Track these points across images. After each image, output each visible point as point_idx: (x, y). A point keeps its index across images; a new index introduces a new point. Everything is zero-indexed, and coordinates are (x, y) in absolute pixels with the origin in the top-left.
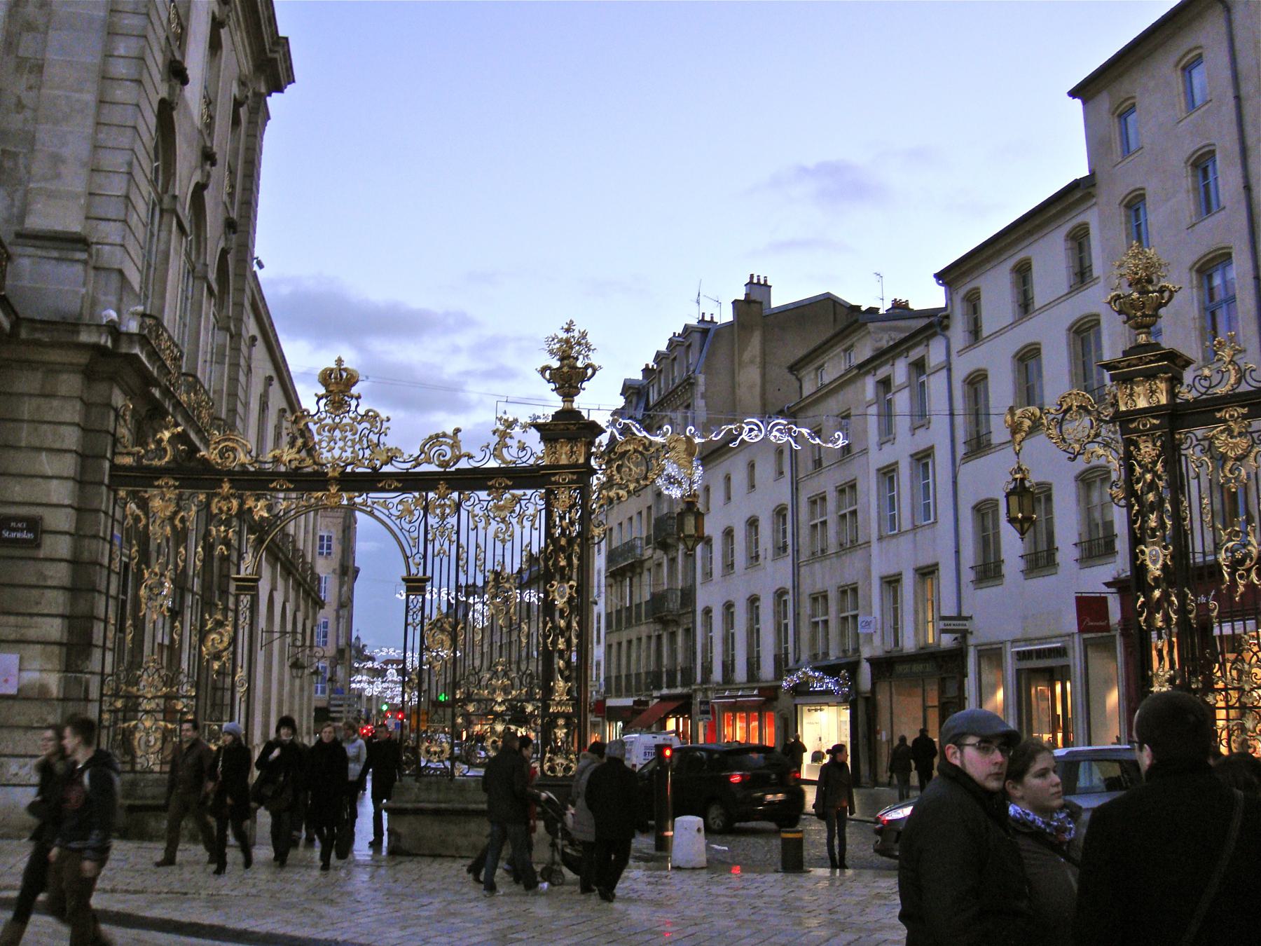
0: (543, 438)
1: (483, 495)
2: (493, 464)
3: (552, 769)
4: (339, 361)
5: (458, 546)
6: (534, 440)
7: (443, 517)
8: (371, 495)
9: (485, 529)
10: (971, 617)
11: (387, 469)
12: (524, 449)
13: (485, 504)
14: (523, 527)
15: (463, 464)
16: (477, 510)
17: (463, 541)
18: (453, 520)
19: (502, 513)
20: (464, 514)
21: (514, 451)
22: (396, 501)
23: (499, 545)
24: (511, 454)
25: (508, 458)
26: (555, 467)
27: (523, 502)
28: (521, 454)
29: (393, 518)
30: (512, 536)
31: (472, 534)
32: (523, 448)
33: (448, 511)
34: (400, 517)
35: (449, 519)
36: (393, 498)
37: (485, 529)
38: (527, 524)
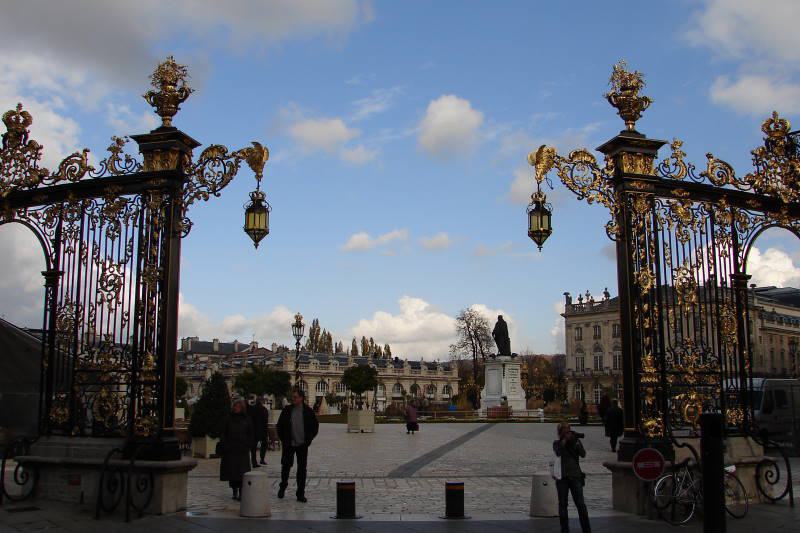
0: (142, 150)
1: (100, 201)
2: (107, 175)
3: (414, 389)
4: (20, 106)
5: (81, 244)
6: (132, 149)
7: (71, 222)
8: (30, 208)
9: (101, 227)
11: (41, 186)
13: (100, 207)
14: (127, 226)
15: (86, 177)
16: (96, 214)
18: (78, 223)
19: (109, 213)
20: (86, 217)
21: (122, 163)
22: (42, 211)
23: (109, 240)
24: (121, 166)
25: (119, 169)
26: (153, 175)
27: (129, 204)
28: (128, 165)
29: (40, 225)
31: (91, 232)
32: (128, 160)
33: (76, 215)
34: (44, 224)
35: (75, 222)
36: (41, 209)
37: (101, 227)
38: (130, 222)
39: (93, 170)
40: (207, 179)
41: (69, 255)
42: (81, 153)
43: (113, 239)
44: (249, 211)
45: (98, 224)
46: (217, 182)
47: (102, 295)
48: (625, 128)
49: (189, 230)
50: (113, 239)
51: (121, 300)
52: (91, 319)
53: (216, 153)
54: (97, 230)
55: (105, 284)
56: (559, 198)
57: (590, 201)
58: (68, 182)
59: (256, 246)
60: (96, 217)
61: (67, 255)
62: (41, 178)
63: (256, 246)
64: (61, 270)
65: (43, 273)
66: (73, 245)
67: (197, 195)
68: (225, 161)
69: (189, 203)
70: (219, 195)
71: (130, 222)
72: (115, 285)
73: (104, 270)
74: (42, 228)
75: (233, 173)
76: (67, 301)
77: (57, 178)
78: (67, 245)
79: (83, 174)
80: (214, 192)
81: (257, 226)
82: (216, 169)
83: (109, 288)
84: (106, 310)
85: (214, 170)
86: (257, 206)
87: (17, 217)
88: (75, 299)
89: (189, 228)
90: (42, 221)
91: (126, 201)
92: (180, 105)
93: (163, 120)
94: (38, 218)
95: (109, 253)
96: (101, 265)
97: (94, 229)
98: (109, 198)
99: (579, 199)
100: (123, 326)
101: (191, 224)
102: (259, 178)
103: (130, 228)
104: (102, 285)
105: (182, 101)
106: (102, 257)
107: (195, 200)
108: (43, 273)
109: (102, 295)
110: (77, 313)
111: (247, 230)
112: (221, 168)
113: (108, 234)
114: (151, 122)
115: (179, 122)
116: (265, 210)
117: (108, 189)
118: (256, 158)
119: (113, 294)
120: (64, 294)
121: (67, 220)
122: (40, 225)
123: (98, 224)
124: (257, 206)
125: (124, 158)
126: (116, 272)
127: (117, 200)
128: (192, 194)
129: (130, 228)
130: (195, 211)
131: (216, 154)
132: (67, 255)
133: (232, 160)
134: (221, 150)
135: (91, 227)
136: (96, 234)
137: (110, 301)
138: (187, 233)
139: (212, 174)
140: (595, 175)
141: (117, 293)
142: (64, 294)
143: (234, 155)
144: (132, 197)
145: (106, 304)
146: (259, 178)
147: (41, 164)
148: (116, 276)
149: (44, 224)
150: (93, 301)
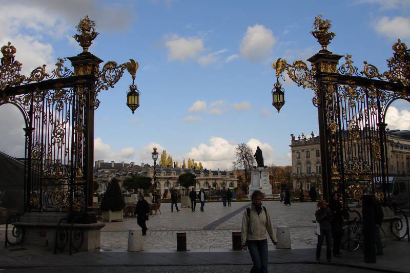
0: (73, 65)
1: (52, 91)
2: (56, 78)
3: (215, 185)
4: (9, 43)
5: (43, 113)
6: (68, 64)
7: (38, 102)
8: (16, 96)
9: (53, 105)
10: (292, 135)
11: (22, 84)
12: (67, 70)
14: (66, 104)
15: (45, 79)
16: (50, 98)
17: (45, 111)
18: (41, 103)
19: (57, 97)
20: (45, 100)
21: (63, 72)
24: (62, 73)
25: (62, 75)
27: (67, 93)
28: (66, 72)
29: (22, 105)
30: (63, 107)
31: (48, 107)
32: (66, 70)
33: (40, 99)
34: (24, 104)
35: (40, 103)
36: (22, 96)
37: (53, 105)
38: (68, 102)
39: (48, 75)
40: (107, 79)
41: (37, 120)
42: (42, 67)
43: (59, 111)
44: (129, 95)
45: (51, 104)
46: (112, 81)
47: (55, 140)
48: (322, 49)
49: (98, 105)
50: (59, 111)
51: (64, 142)
52: (49, 152)
53: (112, 65)
54: (51, 106)
55: (56, 134)
56: (288, 84)
57: (304, 87)
58: (35, 82)
59: (133, 113)
60: (50, 100)
61: (36, 119)
62: (22, 80)
63: (133, 113)
64: (33, 127)
65: (24, 129)
66: (39, 114)
67: (102, 87)
68: (116, 70)
69: (99, 91)
70: (113, 87)
71: (68, 102)
72: (61, 134)
73: (55, 127)
74: (23, 106)
75: (120, 75)
76: (37, 143)
77: (29, 80)
78: (36, 114)
79: (43, 78)
80: (111, 85)
81: (133, 103)
82: (111, 74)
83: (58, 136)
84: (57, 147)
85: (110, 74)
86: (133, 93)
87: (10, 101)
88: (40, 142)
89: (98, 104)
90: (23, 102)
91: (66, 91)
92: (92, 41)
93: (84, 49)
94: (21, 101)
95: (58, 118)
96: (53, 124)
97: (49, 106)
98: (57, 89)
99: (298, 86)
100: (65, 155)
101: (99, 102)
102: (134, 78)
103: (68, 105)
104: (54, 134)
105: (93, 39)
106: (54, 120)
107: (101, 90)
108: (24, 129)
109: (55, 140)
110: (42, 149)
111: (128, 105)
112: (114, 73)
113: (57, 109)
114: (78, 50)
115: (91, 50)
116: (137, 94)
117: (56, 85)
118: (132, 67)
119: (60, 139)
120: (35, 139)
121: (36, 101)
122: (22, 105)
123: (51, 104)
124: (133, 93)
125: (64, 69)
126: (61, 128)
127: (61, 91)
128: (99, 87)
129: (68, 105)
130: (102, 96)
131: (111, 66)
132: (36, 119)
133: (120, 69)
134: (114, 64)
135: (48, 105)
136: (49, 109)
137: (58, 143)
138: (97, 107)
139: (109, 76)
140: (306, 73)
141: (62, 138)
142: (35, 139)
143: (120, 66)
144: (69, 89)
145: (56, 144)
146: (134, 78)
147: (21, 73)
148: (61, 130)
149: (24, 104)
150: (50, 143)
